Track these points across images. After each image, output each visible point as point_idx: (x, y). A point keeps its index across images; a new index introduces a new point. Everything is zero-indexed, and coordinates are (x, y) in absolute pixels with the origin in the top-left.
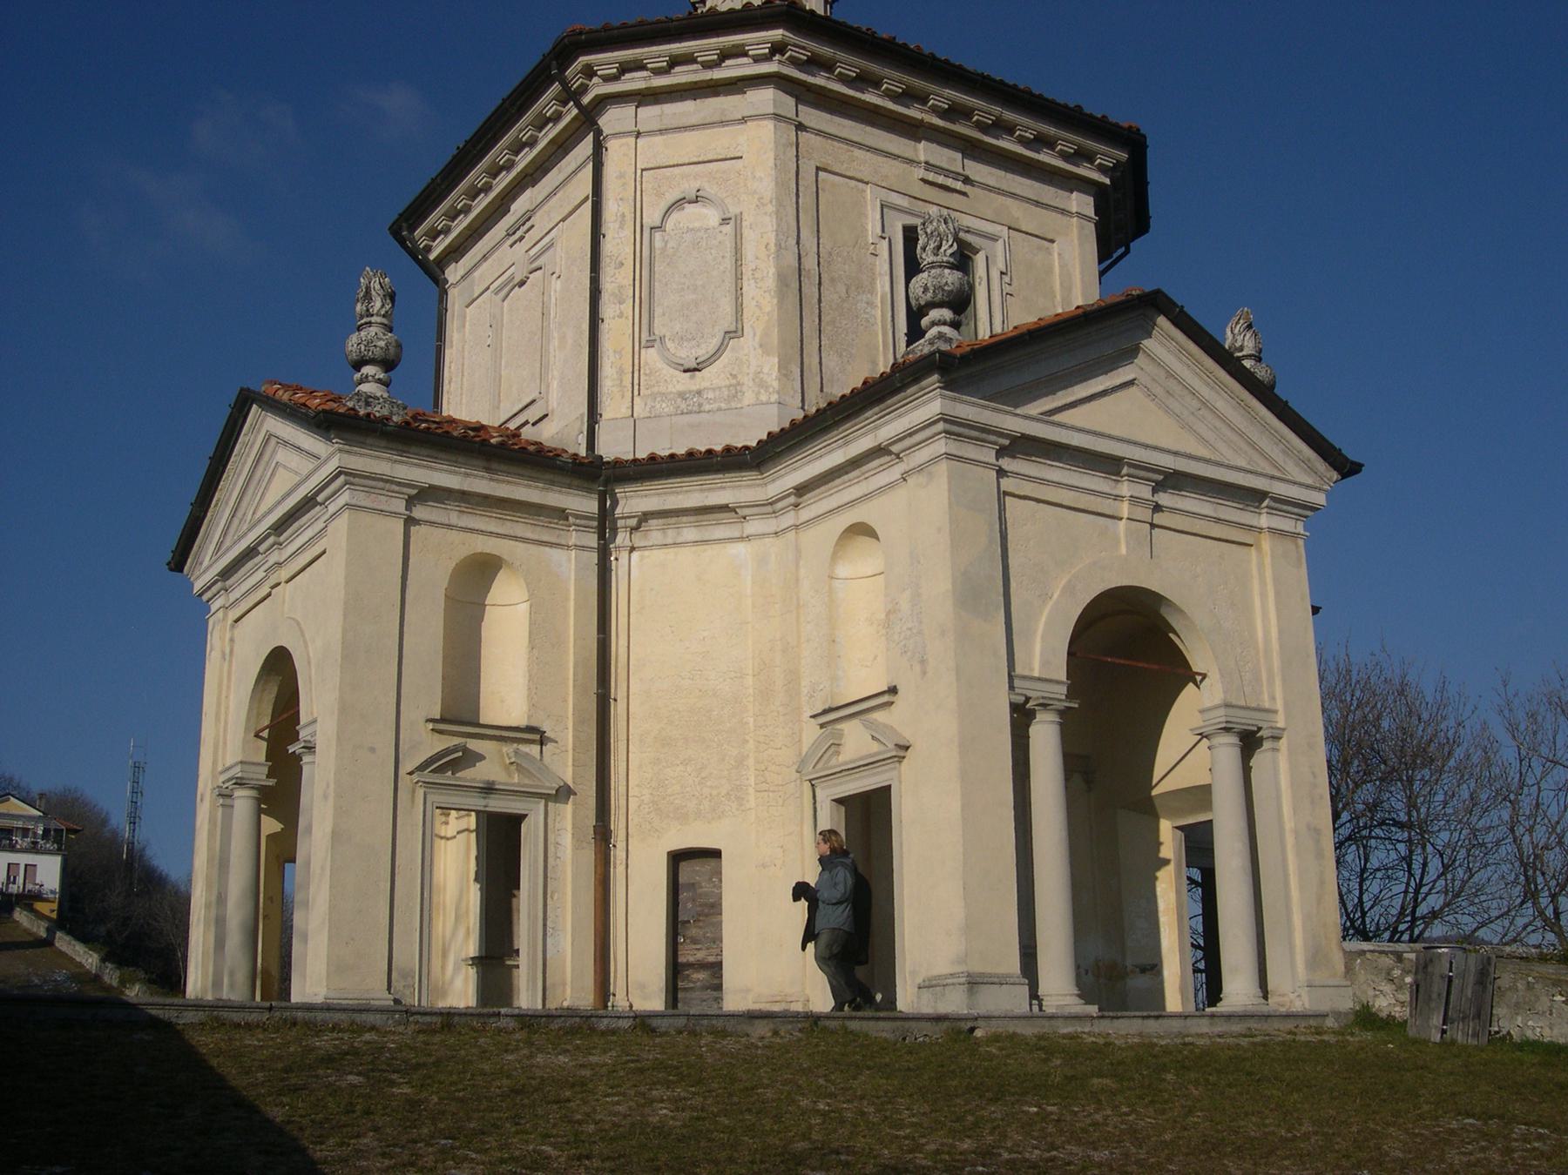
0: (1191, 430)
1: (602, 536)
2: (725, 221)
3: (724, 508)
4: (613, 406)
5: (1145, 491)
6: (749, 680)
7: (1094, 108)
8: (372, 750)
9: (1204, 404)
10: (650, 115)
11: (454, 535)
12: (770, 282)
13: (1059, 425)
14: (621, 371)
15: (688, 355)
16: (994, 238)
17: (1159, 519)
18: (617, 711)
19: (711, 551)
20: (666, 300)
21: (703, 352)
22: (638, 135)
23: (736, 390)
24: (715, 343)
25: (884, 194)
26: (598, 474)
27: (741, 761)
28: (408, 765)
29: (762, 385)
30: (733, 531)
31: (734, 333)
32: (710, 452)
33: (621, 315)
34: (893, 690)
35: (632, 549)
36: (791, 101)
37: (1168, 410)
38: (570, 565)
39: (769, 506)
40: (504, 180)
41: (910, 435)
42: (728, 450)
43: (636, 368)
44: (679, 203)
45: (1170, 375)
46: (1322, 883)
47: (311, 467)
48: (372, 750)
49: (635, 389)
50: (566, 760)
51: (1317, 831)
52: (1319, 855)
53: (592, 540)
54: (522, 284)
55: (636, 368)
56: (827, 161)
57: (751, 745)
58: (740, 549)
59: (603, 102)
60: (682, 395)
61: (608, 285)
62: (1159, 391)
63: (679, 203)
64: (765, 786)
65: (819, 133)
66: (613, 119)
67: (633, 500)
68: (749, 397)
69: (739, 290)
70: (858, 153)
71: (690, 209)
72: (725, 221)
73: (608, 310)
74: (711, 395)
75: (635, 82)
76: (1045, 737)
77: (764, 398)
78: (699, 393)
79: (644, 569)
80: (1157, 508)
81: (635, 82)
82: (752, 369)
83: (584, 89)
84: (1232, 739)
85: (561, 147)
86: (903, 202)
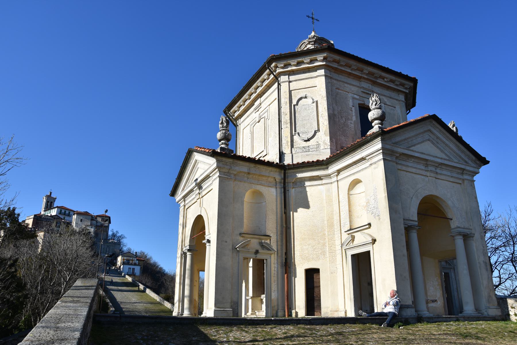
0: (444, 153)
2: (313, 102)
5: (433, 169)
6: (326, 222)
7: (404, 73)
8: (226, 242)
9: (446, 145)
13: (412, 151)
14: (287, 142)
17: (439, 176)
23: (318, 145)
27: (324, 244)
29: (326, 144)
32: (313, 161)
33: (287, 127)
34: (370, 224)
35: (293, 188)
37: (438, 147)
40: (254, 96)
41: (372, 154)
42: (318, 161)
45: (438, 138)
47: (208, 167)
48: (226, 242)
54: (259, 122)
57: (327, 240)
59: (281, 74)
60: (303, 147)
62: (435, 142)
64: (331, 251)
65: (336, 80)
68: (322, 147)
70: (346, 85)
72: (313, 102)
73: (283, 126)
74: (312, 147)
77: (326, 147)
78: (308, 147)
80: (437, 173)
82: (323, 140)
83: (275, 71)
84: (461, 237)
85: (269, 87)
86: (358, 97)
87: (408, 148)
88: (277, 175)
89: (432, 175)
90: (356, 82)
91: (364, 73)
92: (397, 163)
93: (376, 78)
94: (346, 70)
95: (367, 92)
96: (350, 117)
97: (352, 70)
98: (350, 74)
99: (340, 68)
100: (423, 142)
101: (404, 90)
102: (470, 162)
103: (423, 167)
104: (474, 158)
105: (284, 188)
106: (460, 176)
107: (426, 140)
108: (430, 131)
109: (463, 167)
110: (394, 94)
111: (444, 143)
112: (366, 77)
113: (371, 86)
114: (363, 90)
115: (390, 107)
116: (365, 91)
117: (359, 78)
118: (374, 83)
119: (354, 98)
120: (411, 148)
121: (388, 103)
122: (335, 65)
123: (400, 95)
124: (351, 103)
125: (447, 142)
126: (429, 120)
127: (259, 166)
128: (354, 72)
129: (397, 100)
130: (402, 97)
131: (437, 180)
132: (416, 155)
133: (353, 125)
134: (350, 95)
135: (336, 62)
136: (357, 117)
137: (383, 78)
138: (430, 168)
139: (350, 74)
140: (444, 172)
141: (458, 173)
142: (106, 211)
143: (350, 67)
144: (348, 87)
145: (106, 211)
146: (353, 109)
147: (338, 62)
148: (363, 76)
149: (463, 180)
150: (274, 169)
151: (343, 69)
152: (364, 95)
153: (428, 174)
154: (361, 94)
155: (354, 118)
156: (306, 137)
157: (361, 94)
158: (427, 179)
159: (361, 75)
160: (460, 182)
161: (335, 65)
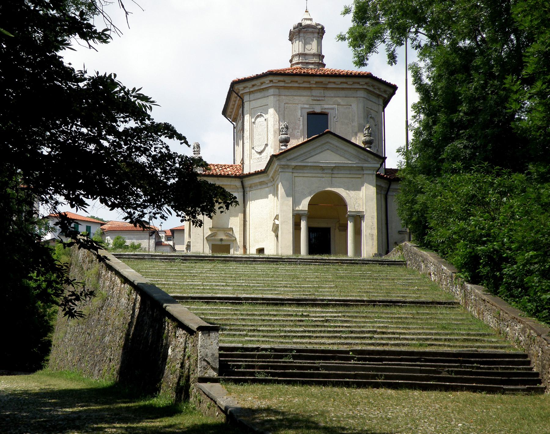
4: (246, 162)
5: (330, 171)
9: (345, 151)
10: (252, 96)
12: (272, 133)
16: (333, 109)
18: (248, 223)
20: (256, 137)
22: (250, 101)
25: (302, 106)
26: (242, 177)
28: (206, 236)
31: (267, 145)
36: (277, 90)
43: (251, 154)
44: (258, 116)
46: (373, 245)
49: (250, 157)
51: (373, 235)
52: (373, 239)
55: (251, 154)
58: (267, 189)
66: (246, 98)
67: (248, 182)
69: (267, 134)
70: (296, 98)
75: (247, 90)
81: (247, 90)
83: (239, 92)
87: (302, 161)
88: (238, 183)
89: (328, 175)
91: (313, 84)
92: (293, 173)
93: (327, 84)
94: (293, 85)
95: (318, 99)
96: (297, 127)
97: (299, 84)
98: (299, 88)
99: (286, 85)
100: (322, 152)
101: (361, 87)
102: (369, 160)
104: (372, 156)
105: (244, 192)
106: (362, 172)
107: (325, 150)
108: (328, 142)
109: (359, 165)
110: (349, 93)
111: (343, 149)
112: (314, 86)
113: (322, 91)
114: (313, 98)
115: (345, 107)
116: (315, 98)
117: (310, 88)
118: (326, 88)
119: (302, 108)
120: (307, 160)
121: (342, 103)
122: (282, 84)
123: (358, 92)
124: (299, 114)
125: (346, 148)
126: (325, 135)
127: (220, 178)
128: (301, 85)
129: (354, 97)
130: (361, 94)
132: (309, 164)
133: (299, 134)
134: (300, 106)
135: (282, 81)
136: (303, 126)
137: (334, 83)
140: (342, 172)
141: (358, 170)
143: (297, 82)
148: (311, 86)
149: (363, 174)
150: (233, 179)
151: (290, 85)
152: (315, 102)
153: (324, 175)
154: (311, 102)
155: (301, 127)
156: (259, 151)
157: (311, 102)
158: (323, 179)
159: (309, 86)
160: (360, 176)
161: (282, 84)
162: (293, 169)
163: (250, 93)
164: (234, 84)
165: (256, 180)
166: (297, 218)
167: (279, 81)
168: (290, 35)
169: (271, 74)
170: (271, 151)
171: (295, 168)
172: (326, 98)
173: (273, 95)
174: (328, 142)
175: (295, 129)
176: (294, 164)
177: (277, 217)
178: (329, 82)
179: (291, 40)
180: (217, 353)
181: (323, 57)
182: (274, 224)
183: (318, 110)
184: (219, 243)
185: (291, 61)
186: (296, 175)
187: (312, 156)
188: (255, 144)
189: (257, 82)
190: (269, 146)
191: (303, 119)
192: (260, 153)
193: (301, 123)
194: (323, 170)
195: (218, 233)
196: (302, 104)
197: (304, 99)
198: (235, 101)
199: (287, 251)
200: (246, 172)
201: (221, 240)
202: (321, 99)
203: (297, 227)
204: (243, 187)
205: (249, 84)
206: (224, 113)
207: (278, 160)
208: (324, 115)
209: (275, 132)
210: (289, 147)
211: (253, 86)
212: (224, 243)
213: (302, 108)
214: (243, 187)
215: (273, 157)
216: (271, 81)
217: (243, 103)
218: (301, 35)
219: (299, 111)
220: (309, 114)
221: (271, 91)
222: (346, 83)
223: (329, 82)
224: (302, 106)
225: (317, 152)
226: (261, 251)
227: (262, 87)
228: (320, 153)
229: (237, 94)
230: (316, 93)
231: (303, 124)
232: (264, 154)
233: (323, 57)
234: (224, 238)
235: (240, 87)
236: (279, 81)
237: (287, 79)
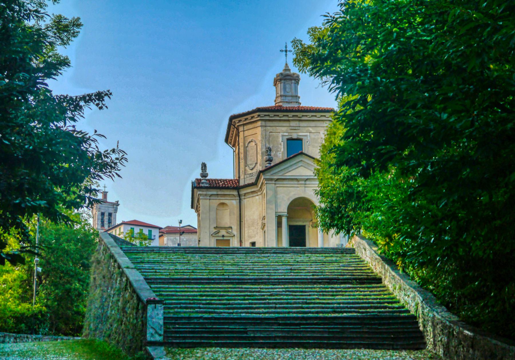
1: (240, 197)
3: (254, 191)
4: (242, 177)
5: (303, 182)
10: (246, 127)
11: (217, 201)
15: (251, 167)
17: (306, 186)
19: (254, 198)
20: (249, 158)
21: (253, 166)
22: (244, 131)
24: (254, 165)
30: (256, 194)
31: (256, 163)
38: (234, 203)
39: (259, 191)
43: (245, 170)
44: (250, 142)
49: (245, 174)
50: (235, 231)
53: (238, 198)
55: (245, 170)
56: (271, 131)
58: (257, 197)
59: (238, 126)
61: (241, 157)
63: (250, 142)
66: (241, 129)
67: (243, 192)
70: (278, 128)
71: (251, 143)
73: (241, 161)
76: (284, 220)
79: (246, 202)
88: (235, 193)
90: (286, 124)
95: (295, 128)
96: (279, 150)
97: (280, 117)
98: (280, 120)
100: (297, 168)
103: (296, 183)
105: (240, 200)
116: (293, 128)
117: (288, 120)
119: (283, 136)
120: (286, 175)
121: (313, 131)
122: (267, 118)
124: (281, 139)
128: (282, 119)
131: (306, 188)
134: (281, 134)
138: (300, 182)
139: (280, 120)
142: (181, 222)
144: (279, 129)
145: (181, 222)
146: (282, 143)
147: (269, 115)
153: (299, 186)
154: (290, 131)
155: (282, 150)
157: (290, 131)
158: (298, 189)
161: (267, 118)
162: (275, 181)
163: (244, 125)
164: (232, 118)
165: (249, 190)
166: (279, 218)
167: (265, 115)
168: (274, 81)
169: (259, 110)
170: (259, 168)
171: (278, 179)
172: (300, 128)
173: (261, 126)
174: (301, 161)
175: (278, 151)
176: (276, 177)
177: (264, 218)
178: (303, 116)
179: (275, 85)
180: (161, 322)
181: (299, 97)
182: (262, 223)
183: (295, 136)
184: (222, 238)
185: (275, 101)
186: (278, 185)
187: (289, 171)
188: (249, 162)
189: (249, 117)
190: (258, 164)
191: (284, 144)
192: (252, 169)
193: (282, 147)
194: (299, 181)
195: (221, 230)
196: (282, 132)
197: (284, 129)
198: (233, 131)
199: (272, 244)
200: (242, 183)
201: (223, 236)
202: (297, 128)
203: (279, 225)
204: (239, 195)
205: (243, 118)
206: (226, 140)
207: (264, 174)
208: (300, 140)
209: (262, 153)
210: (272, 165)
211: (246, 119)
212: (225, 238)
213: (283, 136)
214: (239, 195)
215: (261, 172)
216: (259, 116)
217: (239, 132)
218: (283, 81)
219: (281, 138)
220: (288, 140)
221: (259, 123)
222: (316, 116)
223: (303, 116)
224: (283, 134)
225: (294, 168)
226: (253, 244)
227: (252, 120)
228: (295, 169)
229: (234, 126)
230: (293, 124)
231: (284, 147)
232: (255, 170)
233: (299, 97)
234: (225, 234)
235: (236, 120)
236: (265, 115)
237: (272, 114)
